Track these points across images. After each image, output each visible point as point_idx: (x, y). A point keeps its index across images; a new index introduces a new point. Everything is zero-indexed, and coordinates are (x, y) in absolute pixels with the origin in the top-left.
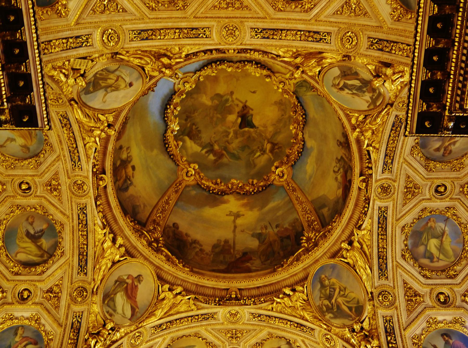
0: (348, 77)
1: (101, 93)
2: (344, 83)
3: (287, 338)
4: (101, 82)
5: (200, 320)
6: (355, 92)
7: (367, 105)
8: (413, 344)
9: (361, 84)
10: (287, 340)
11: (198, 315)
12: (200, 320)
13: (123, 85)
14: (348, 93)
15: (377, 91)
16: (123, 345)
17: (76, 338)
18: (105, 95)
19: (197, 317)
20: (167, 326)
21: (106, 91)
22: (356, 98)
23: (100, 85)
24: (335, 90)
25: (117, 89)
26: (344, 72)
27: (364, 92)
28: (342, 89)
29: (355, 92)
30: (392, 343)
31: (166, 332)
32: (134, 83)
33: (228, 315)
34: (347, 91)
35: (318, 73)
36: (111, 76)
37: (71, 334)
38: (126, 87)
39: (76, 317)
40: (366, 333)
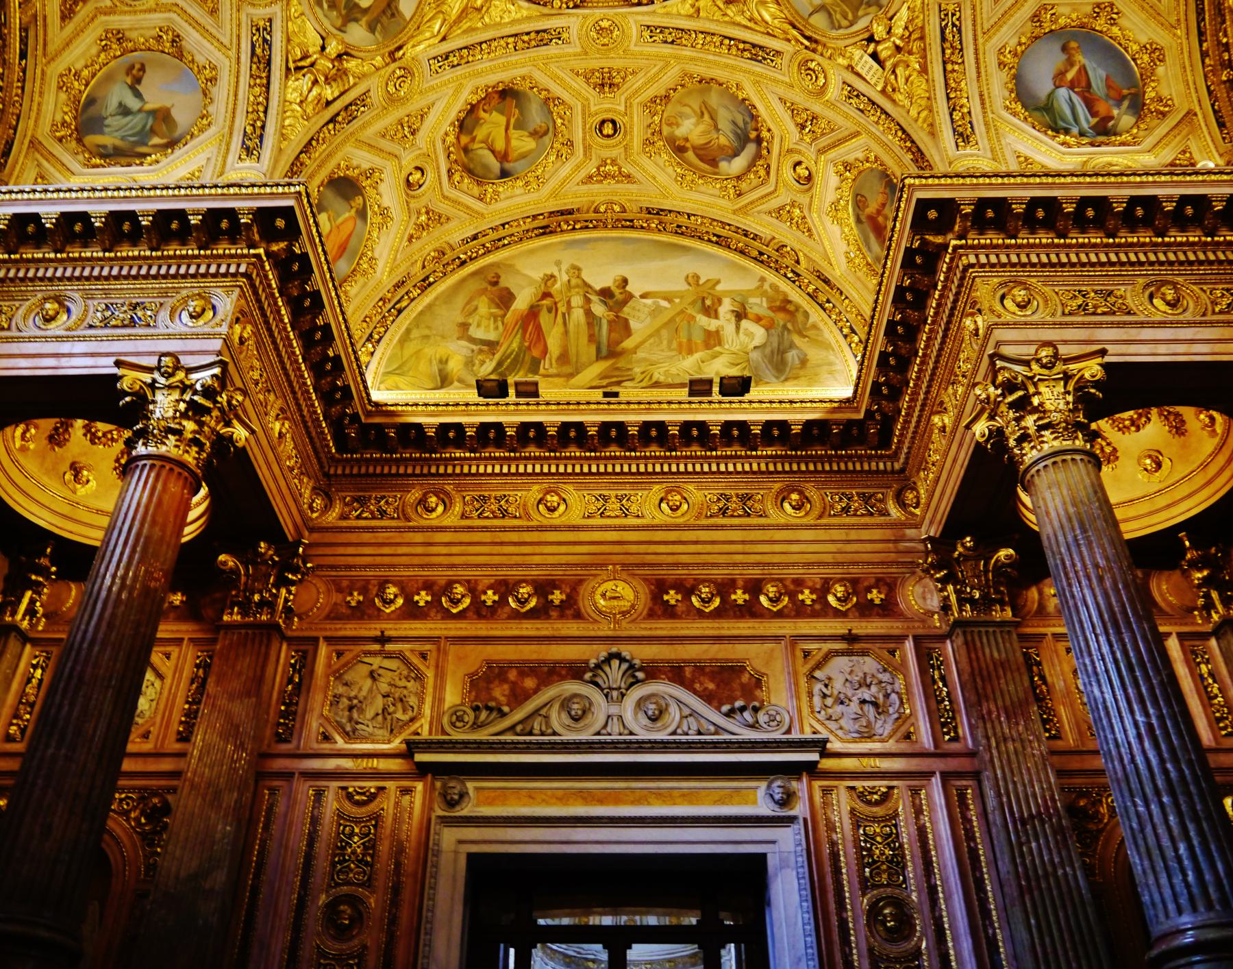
3: (722, 80)
5: (533, 43)
8: (1000, 64)
10: (721, 85)
11: (528, 34)
12: (533, 43)
16: (371, 93)
17: (264, 75)
19: (526, 38)
20: (462, 57)
30: (953, 63)
31: (459, 71)
33: (593, 34)
37: (254, 66)
39: (258, 30)
40: (898, 42)
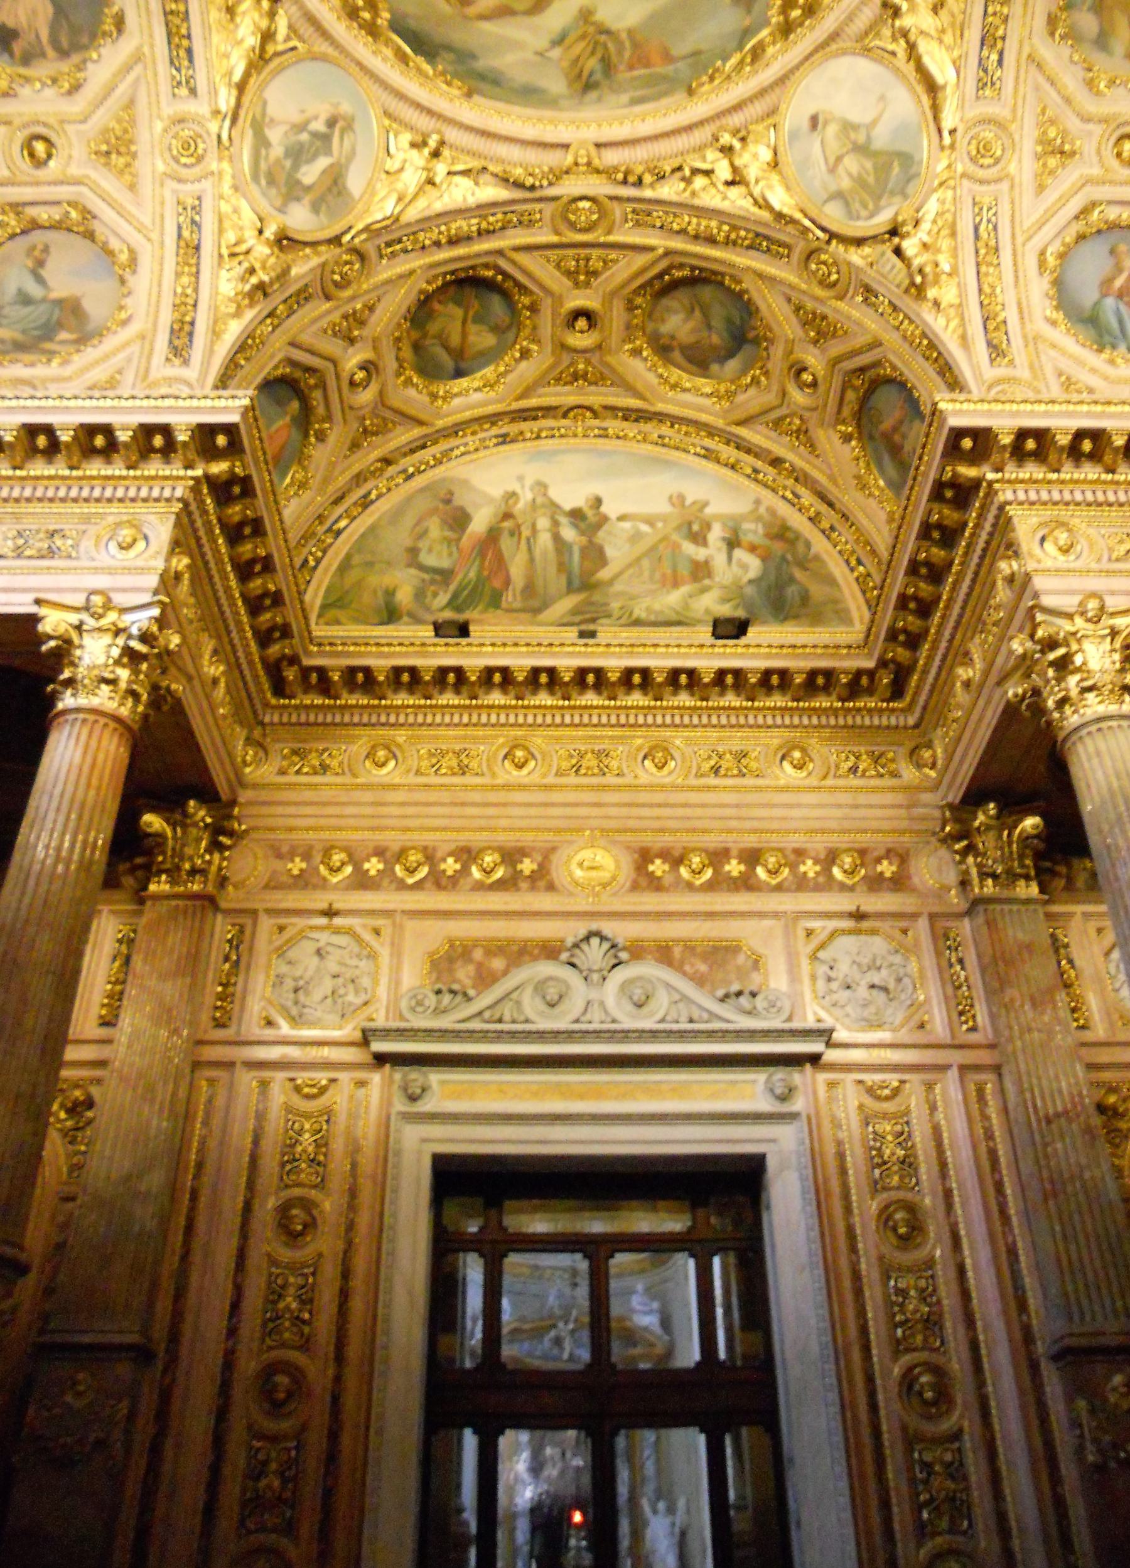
0: (328, 182)
1: (881, 139)
2: (328, 152)
4: (871, 180)
6: (304, 137)
7: (271, 111)
9: (299, 176)
13: (832, 130)
14: (316, 118)
15: (263, 182)
18: (874, 123)
21: (869, 138)
22: (297, 118)
23: (875, 168)
24: (346, 108)
25: (848, 127)
26: (339, 193)
27: (288, 153)
28: (332, 123)
29: (304, 137)
32: (806, 124)
34: (319, 126)
35: (392, 150)
36: (846, 184)
38: (826, 123)
